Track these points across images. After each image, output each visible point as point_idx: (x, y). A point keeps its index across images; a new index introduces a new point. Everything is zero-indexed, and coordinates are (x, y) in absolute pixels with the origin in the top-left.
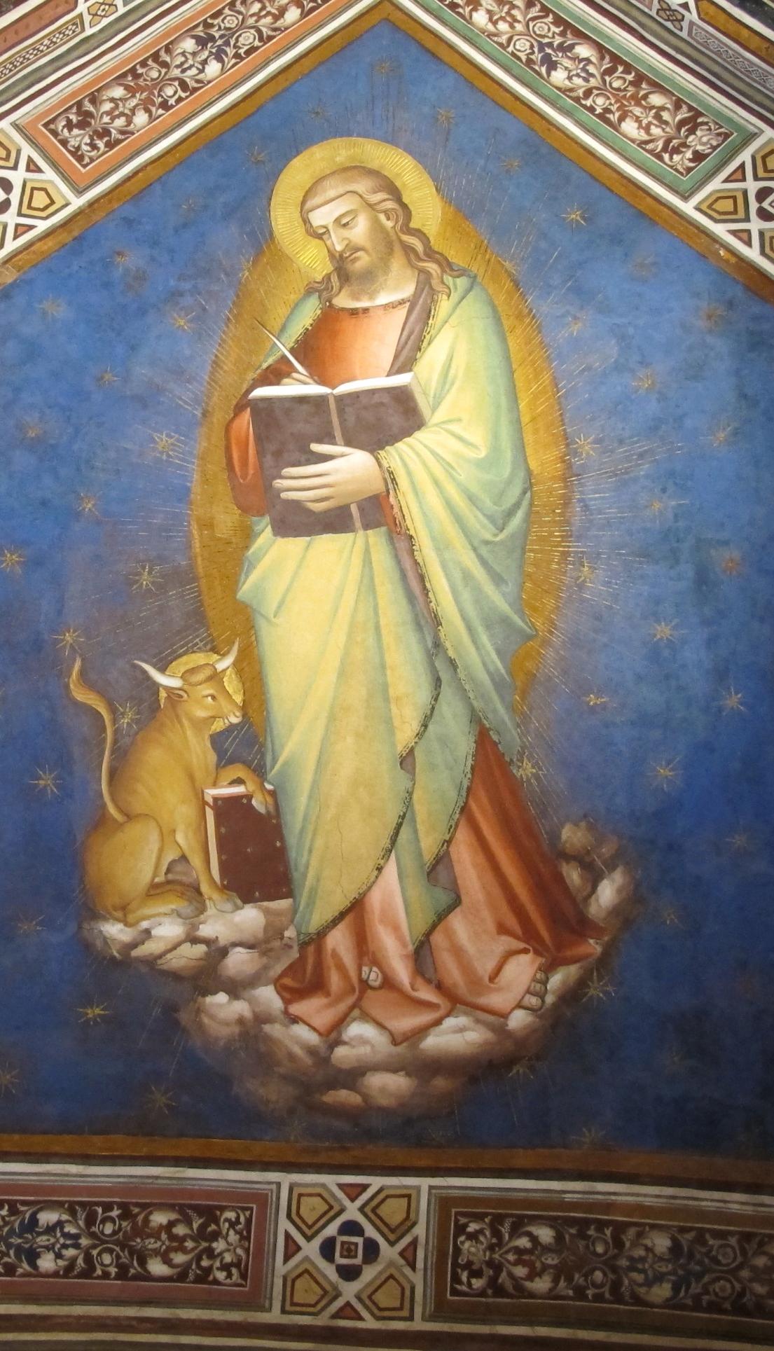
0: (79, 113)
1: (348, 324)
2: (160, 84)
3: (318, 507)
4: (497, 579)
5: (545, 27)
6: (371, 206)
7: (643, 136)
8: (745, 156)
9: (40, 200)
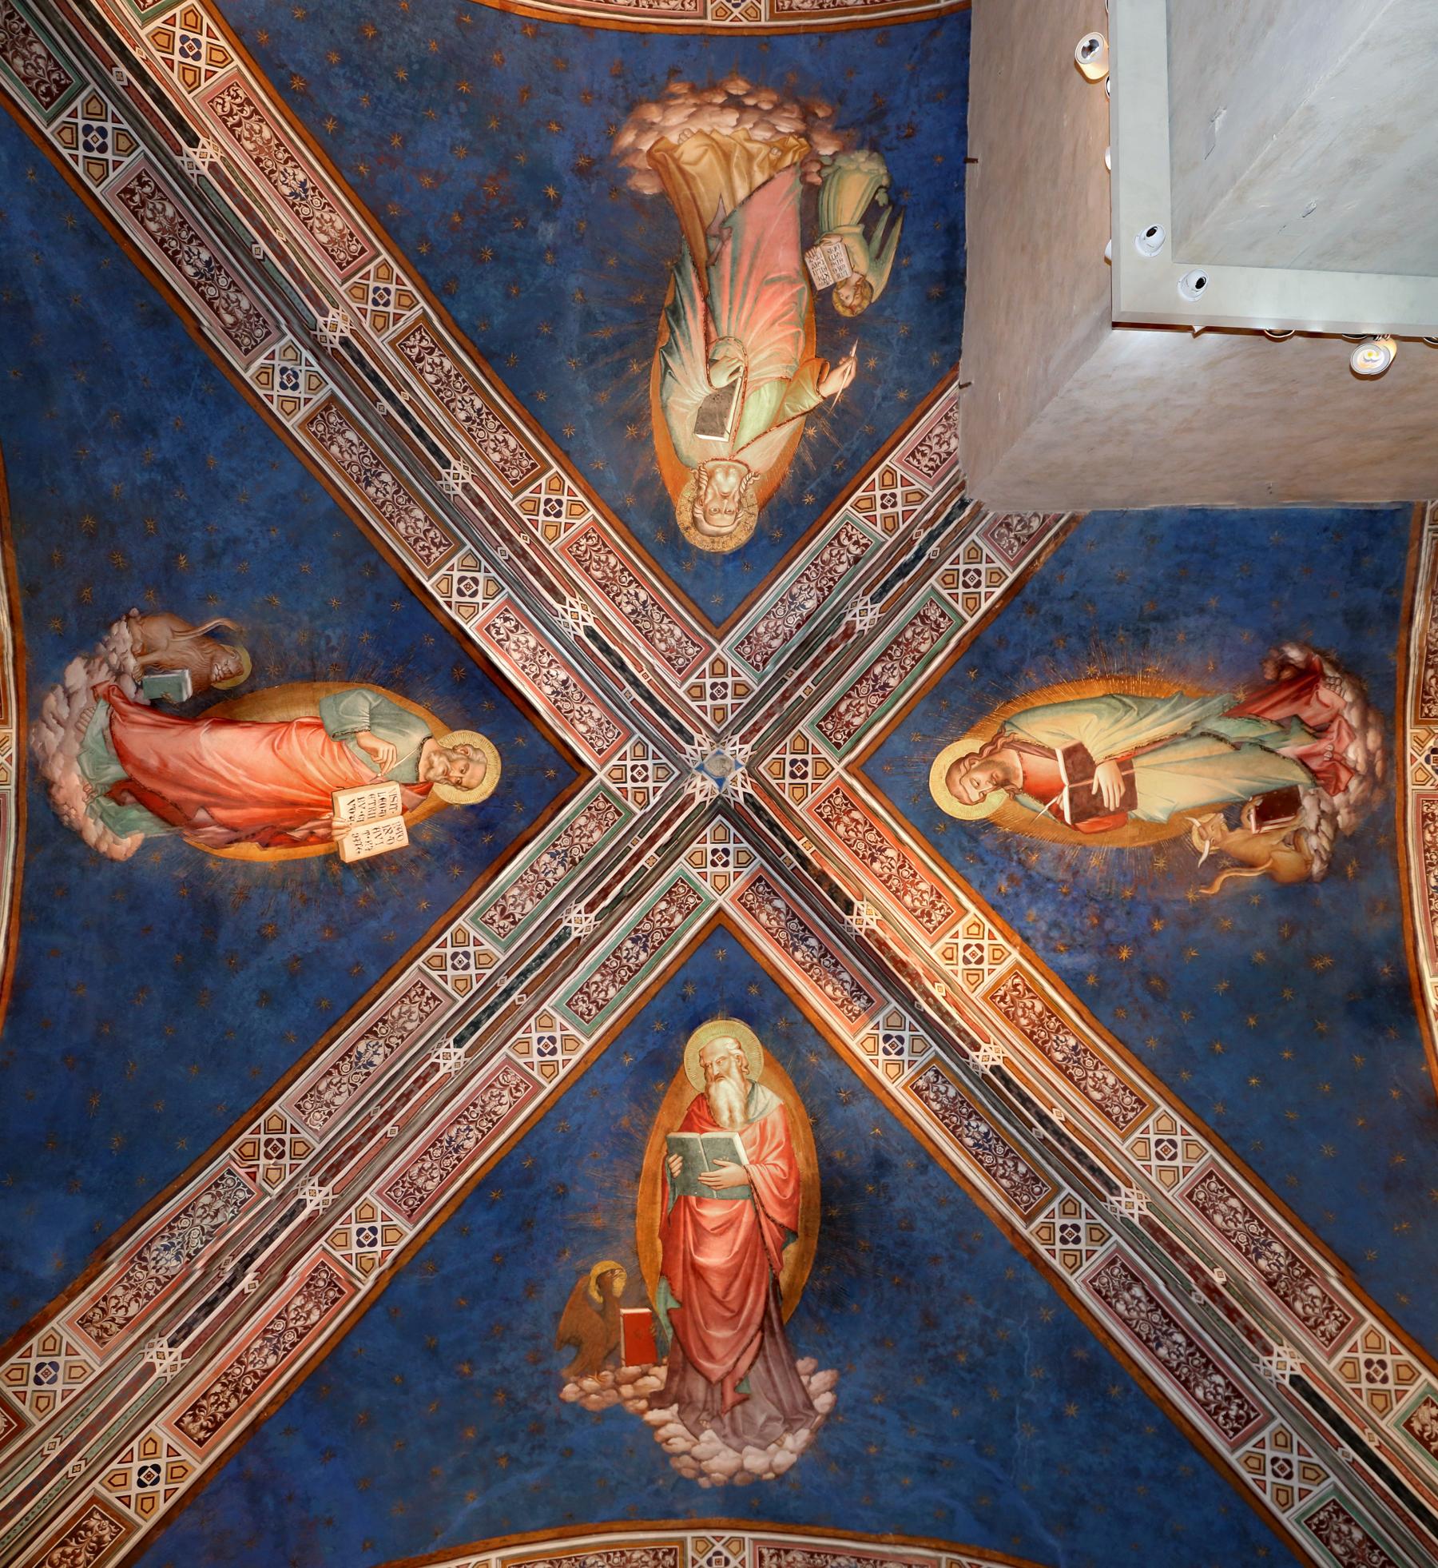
1: (1031, 780)
2: (901, 879)
3: (1123, 790)
4: (1154, 709)
5: (863, 689)
6: (968, 772)
7: (929, 642)
8: (944, 593)
9: (975, 930)
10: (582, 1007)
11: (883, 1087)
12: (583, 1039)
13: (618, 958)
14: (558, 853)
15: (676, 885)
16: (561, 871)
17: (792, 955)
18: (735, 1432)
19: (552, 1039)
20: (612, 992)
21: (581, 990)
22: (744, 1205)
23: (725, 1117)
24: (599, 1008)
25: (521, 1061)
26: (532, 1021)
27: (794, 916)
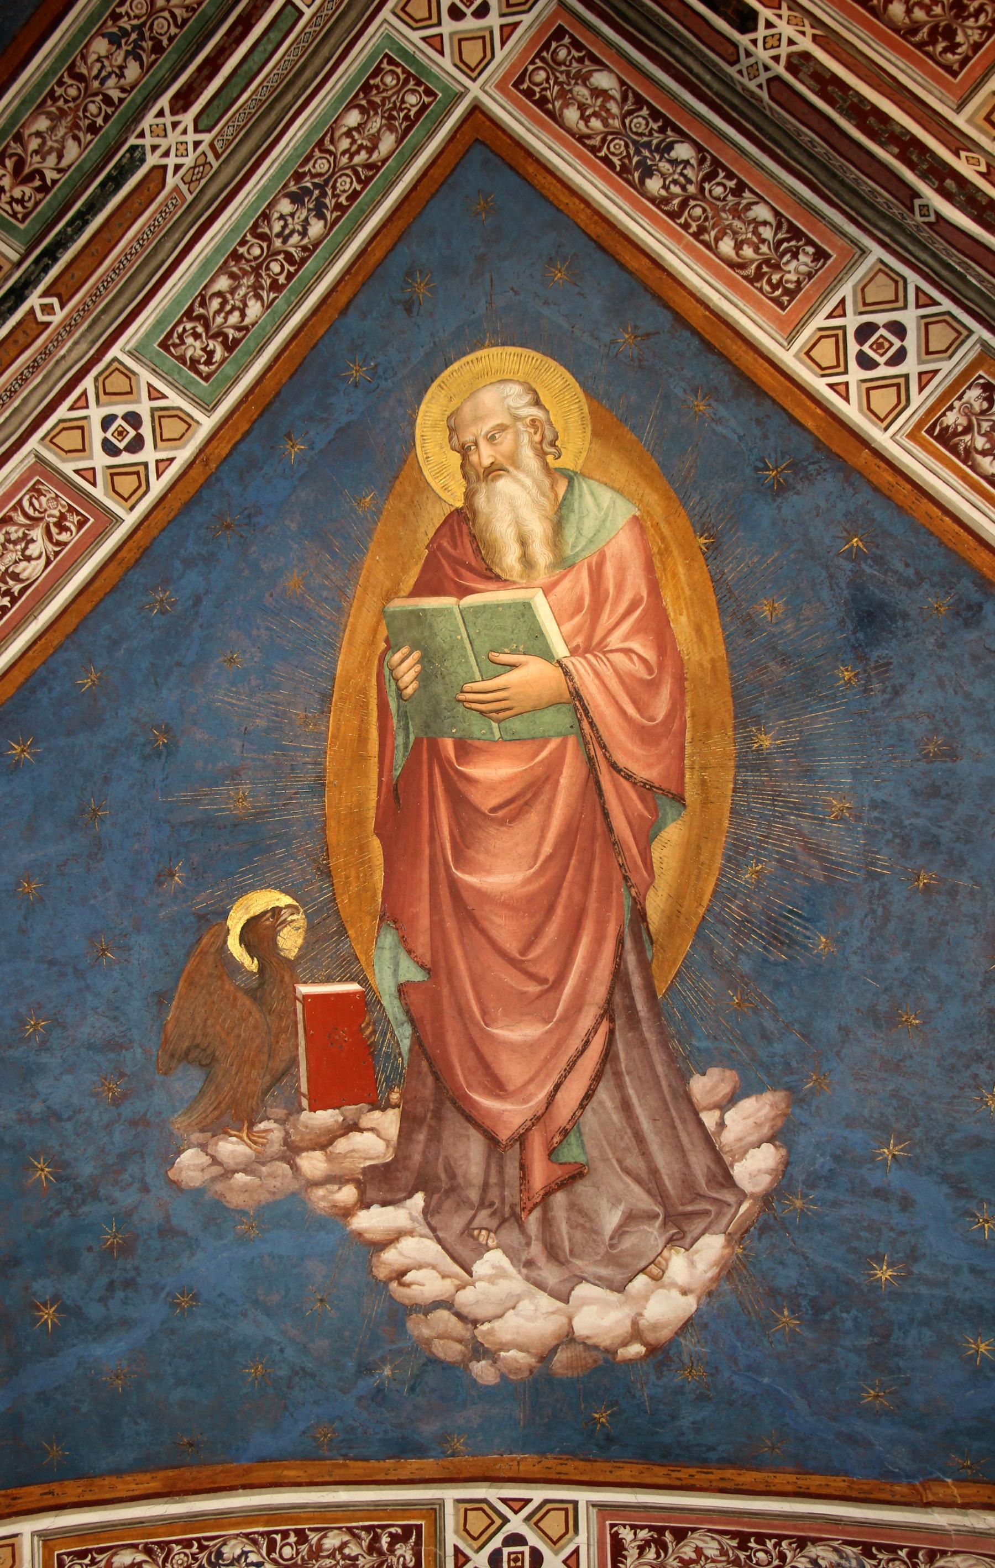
0: (933, 42)
10: (193, 348)
11: (863, 442)
12: (197, 414)
13: (263, 237)
14: (125, 33)
15: (378, 71)
16: (133, 71)
17: (640, 187)
18: (553, 1252)
19: (133, 419)
20: (254, 309)
21: (189, 314)
22: (563, 745)
23: (510, 558)
24: (230, 346)
25: (68, 468)
26: (88, 383)
27: (640, 102)
